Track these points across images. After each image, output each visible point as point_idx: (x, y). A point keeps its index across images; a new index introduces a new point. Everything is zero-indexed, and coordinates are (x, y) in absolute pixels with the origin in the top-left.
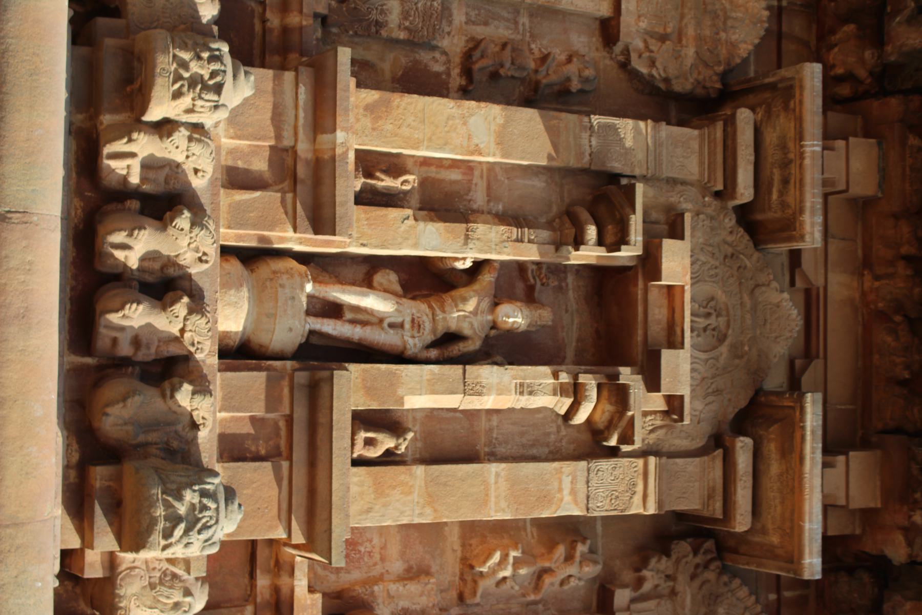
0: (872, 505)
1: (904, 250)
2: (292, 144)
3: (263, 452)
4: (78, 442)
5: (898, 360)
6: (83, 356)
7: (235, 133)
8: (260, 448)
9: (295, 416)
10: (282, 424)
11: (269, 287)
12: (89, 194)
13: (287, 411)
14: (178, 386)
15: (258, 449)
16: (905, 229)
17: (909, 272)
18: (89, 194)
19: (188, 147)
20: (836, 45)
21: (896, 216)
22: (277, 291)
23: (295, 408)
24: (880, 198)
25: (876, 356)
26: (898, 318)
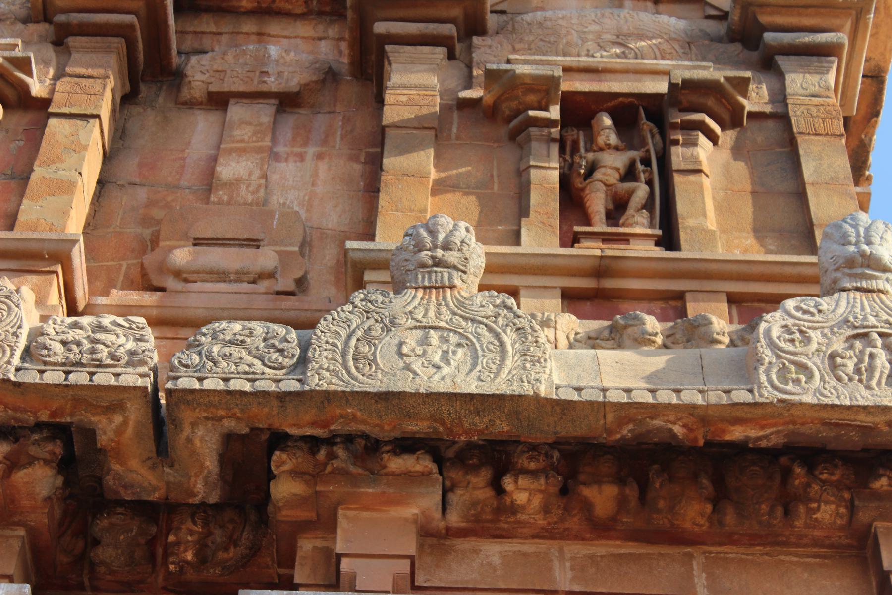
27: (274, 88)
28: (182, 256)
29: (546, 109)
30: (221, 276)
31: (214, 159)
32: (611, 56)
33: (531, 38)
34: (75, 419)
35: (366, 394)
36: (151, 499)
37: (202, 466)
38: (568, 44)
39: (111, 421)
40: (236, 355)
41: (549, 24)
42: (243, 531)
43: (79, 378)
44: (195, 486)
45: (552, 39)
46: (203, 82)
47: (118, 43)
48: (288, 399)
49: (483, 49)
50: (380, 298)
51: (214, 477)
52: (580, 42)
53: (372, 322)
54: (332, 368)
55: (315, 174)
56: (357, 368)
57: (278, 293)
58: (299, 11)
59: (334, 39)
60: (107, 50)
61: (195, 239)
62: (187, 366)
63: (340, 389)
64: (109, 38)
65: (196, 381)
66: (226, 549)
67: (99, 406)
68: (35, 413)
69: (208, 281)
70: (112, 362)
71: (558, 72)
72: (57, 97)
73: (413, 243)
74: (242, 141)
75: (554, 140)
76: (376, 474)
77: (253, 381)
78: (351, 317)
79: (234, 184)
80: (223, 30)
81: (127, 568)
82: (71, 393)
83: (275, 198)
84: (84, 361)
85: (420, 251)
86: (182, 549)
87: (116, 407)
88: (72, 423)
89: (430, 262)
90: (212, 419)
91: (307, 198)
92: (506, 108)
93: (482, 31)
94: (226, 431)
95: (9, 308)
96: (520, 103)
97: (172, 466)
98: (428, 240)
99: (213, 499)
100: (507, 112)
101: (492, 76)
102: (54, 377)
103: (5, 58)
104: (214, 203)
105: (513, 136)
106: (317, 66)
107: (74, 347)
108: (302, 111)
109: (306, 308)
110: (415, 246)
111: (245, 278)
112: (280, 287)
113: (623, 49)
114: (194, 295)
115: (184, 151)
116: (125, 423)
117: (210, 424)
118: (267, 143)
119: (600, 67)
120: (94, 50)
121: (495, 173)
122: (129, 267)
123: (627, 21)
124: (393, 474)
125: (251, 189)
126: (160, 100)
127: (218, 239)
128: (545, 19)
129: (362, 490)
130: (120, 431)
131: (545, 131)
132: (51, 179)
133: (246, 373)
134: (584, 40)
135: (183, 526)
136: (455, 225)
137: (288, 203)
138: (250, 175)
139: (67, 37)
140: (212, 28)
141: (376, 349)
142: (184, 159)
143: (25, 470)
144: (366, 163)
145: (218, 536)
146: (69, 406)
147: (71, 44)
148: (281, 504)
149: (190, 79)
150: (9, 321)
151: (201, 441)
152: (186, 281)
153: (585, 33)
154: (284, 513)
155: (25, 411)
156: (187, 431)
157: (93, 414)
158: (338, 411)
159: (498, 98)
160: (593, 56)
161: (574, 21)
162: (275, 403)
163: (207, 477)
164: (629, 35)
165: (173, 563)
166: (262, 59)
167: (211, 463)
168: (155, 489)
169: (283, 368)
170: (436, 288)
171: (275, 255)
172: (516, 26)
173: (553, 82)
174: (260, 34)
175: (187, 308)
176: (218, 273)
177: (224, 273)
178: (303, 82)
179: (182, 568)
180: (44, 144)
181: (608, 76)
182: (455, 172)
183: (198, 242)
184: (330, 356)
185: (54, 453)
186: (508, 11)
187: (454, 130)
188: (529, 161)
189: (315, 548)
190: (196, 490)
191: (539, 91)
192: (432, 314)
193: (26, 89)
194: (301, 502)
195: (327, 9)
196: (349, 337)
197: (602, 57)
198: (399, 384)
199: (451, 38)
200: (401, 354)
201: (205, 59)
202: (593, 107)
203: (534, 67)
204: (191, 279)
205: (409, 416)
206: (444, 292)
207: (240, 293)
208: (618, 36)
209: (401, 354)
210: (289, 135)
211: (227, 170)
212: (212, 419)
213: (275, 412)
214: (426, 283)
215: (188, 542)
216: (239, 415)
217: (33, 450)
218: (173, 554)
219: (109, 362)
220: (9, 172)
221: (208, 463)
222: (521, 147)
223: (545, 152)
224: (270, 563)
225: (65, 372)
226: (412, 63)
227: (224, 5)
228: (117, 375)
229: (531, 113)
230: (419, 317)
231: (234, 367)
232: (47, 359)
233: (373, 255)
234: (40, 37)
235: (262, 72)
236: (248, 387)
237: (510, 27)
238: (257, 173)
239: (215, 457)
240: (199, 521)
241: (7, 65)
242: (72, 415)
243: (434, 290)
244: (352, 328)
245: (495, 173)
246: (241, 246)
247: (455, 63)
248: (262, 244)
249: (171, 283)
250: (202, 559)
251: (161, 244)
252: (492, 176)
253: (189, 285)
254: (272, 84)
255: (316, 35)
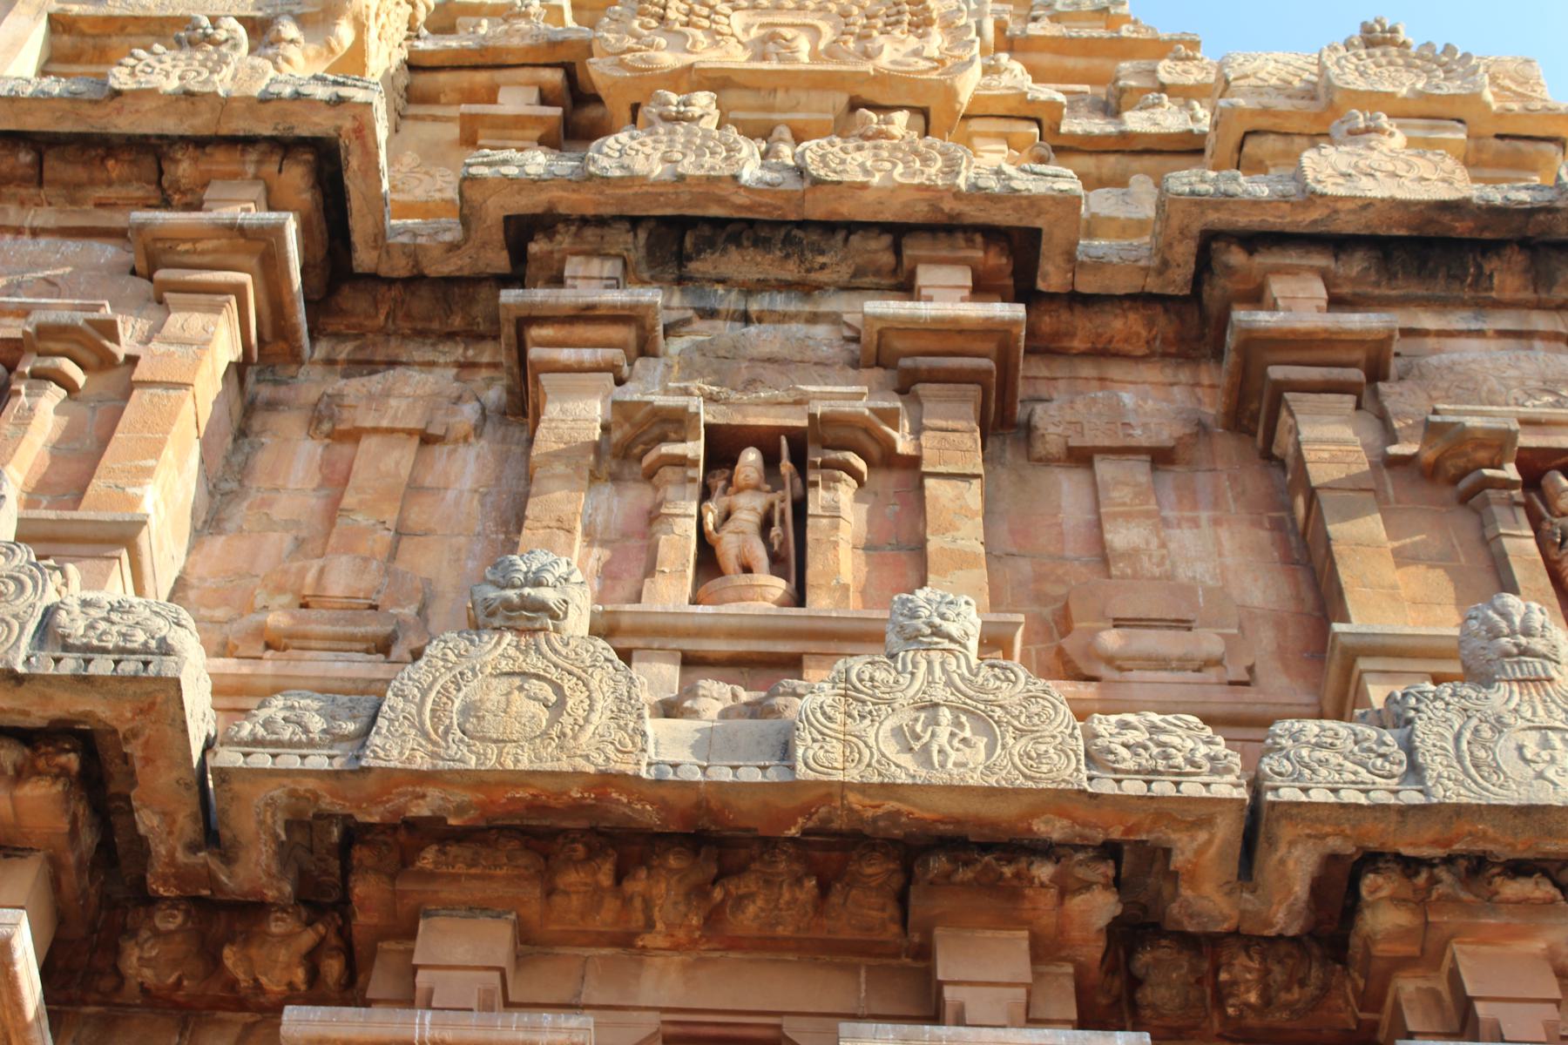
0: (1025, 945)
1: (605, 878)
5: (786, 896)
16: (572, 878)
17: (643, 874)
20: (256, 980)
21: (550, 892)
24: (518, 916)
25: (779, 930)
26: (718, 894)
27: (1145, 443)
28: (1111, 640)
29: (1499, 467)
30: (1160, 663)
31: (1098, 525)
32: (1545, 405)
33: (1446, 385)
34: (1152, 837)
35: (1505, 807)
36: (1218, 930)
37: (1290, 892)
38: (1491, 391)
39: (1193, 839)
40: (1333, 761)
41: (1459, 368)
42: (1310, 968)
43: (1163, 788)
44: (1275, 915)
45: (1470, 385)
46: (1059, 435)
47: (974, 391)
48: (1411, 813)
49: (1393, 398)
50: (1474, 695)
51: (1301, 905)
52: (1503, 389)
53: (1474, 722)
54: (1453, 777)
55: (1218, 542)
56: (1482, 777)
57: (1231, 683)
58: (1139, 353)
59: (1186, 384)
60: (964, 399)
61: (1115, 620)
62: (1280, 774)
63: (1474, 802)
64: (964, 386)
65: (1300, 792)
66: (1288, 989)
67: (1184, 822)
68: (1106, 830)
69: (1146, 669)
70: (1193, 770)
71: (1515, 426)
72: (926, 453)
73: (1484, 628)
74: (1124, 504)
75: (1518, 504)
76: (1492, 901)
77: (1365, 792)
78: (1448, 715)
79: (1132, 555)
80: (1059, 375)
81: (1179, 1012)
82: (1155, 805)
83: (1180, 570)
84: (1161, 768)
85: (1497, 637)
86: (1242, 989)
87: (1205, 822)
88: (1147, 841)
89: (1515, 651)
90: (1315, 837)
91: (1218, 571)
92: (1451, 467)
93: (1385, 378)
94: (1328, 851)
95: (1054, 706)
96: (1469, 461)
97: (1253, 891)
98: (1503, 624)
99: (1293, 931)
100: (1452, 471)
101: (1433, 430)
102: (1133, 787)
103: (871, 409)
104: (1117, 577)
105: (1464, 499)
106: (1184, 416)
107: (1141, 751)
108: (1177, 468)
109: (1274, 701)
110: (1488, 631)
111: (1189, 665)
112: (1232, 677)
113: (1555, 398)
114: (1135, 686)
115: (1055, 515)
116: (1209, 842)
117: (1310, 843)
118: (1153, 506)
119: (1544, 418)
120: (948, 399)
121: (1455, 542)
122: (1038, 653)
123: (1547, 366)
124: (1508, 902)
125: (1154, 560)
126: (1008, 456)
127: (1141, 620)
128: (1454, 363)
129: (1483, 921)
130: (1200, 852)
131: (1505, 493)
132: (952, 551)
133: (1353, 783)
134: (1508, 388)
135: (1236, 962)
136: (1527, 607)
137: (1198, 576)
138: (1148, 543)
139: (915, 383)
140: (1045, 373)
141: (1494, 754)
142: (1060, 525)
143: (1082, 897)
144: (1272, 530)
145: (1278, 974)
146: (1148, 821)
147: (920, 392)
148: (1379, 937)
149: (1041, 432)
150: (1059, 720)
151: (1296, 864)
152: (1120, 669)
153: (1504, 378)
154: (1380, 947)
155: (1095, 826)
156: (1282, 850)
157: (1174, 831)
158: (1467, 828)
159: (1442, 455)
160: (1523, 405)
161: (1488, 365)
162: (1394, 817)
163: (1293, 904)
164: (1558, 381)
165: (1232, 1006)
166: (1118, 408)
167: (1301, 889)
168: (1226, 918)
169: (1392, 776)
170: (1532, 681)
171: (1219, 638)
172: (1424, 370)
173: (1510, 436)
174: (1101, 379)
175: (1133, 701)
176: (1157, 660)
177: (1164, 660)
178: (1176, 435)
179: (1241, 1011)
180: (928, 508)
181: (1554, 429)
182: (1408, 541)
183: (1118, 623)
184: (1445, 763)
185: (1107, 876)
186: (1403, 353)
187: (1391, 491)
188: (1497, 529)
189: (1418, 989)
190: (1275, 920)
191: (1491, 446)
192: (1540, 711)
193: (890, 444)
194: (1404, 934)
195: (1173, 350)
196: (1457, 738)
197: (1534, 406)
198: (1541, 796)
199: (1359, 384)
200: (1527, 761)
201: (1052, 408)
202: (1539, 465)
203: (1485, 419)
204: (1126, 667)
205: (1550, 834)
206: (1543, 685)
207: (1188, 683)
208: (1545, 383)
209: (1527, 761)
210: (1173, 497)
211: (1120, 537)
212: (1315, 837)
213: (1392, 829)
214: (1519, 675)
215: (1247, 981)
216: (1348, 832)
217: (1081, 872)
218: (1231, 995)
219: (1189, 769)
220: (894, 542)
221: (1297, 888)
222: (1477, 511)
223: (1511, 519)
224: (1343, 1006)
225: (1146, 781)
226: (1319, 413)
227: (1053, 346)
228: (1207, 785)
229: (1487, 472)
230: (1528, 715)
231: (1337, 776)
232: (1116, 766)
233: (1367, 640)
234: (880, 384)
235: (1124, 424)
236: (1363, 800)
237: (1416, 371)
238: (1155, 542)
239: (1308, 881)
240: (1256, 957)
241: (873, 418)
242: (1149, 832)
243: (1515, 687)
244: (1456, 727)
245: (1455, 542)
246: (1169, 627)
247: (1361, 413)
248: (1194, 625)
249: (1103, 670)
250: (1267, 1001)
251: (1077, 625)
252: (1453, 546)
253: (1126, 673)
254: (1140, 437)
255: (1166, 380)
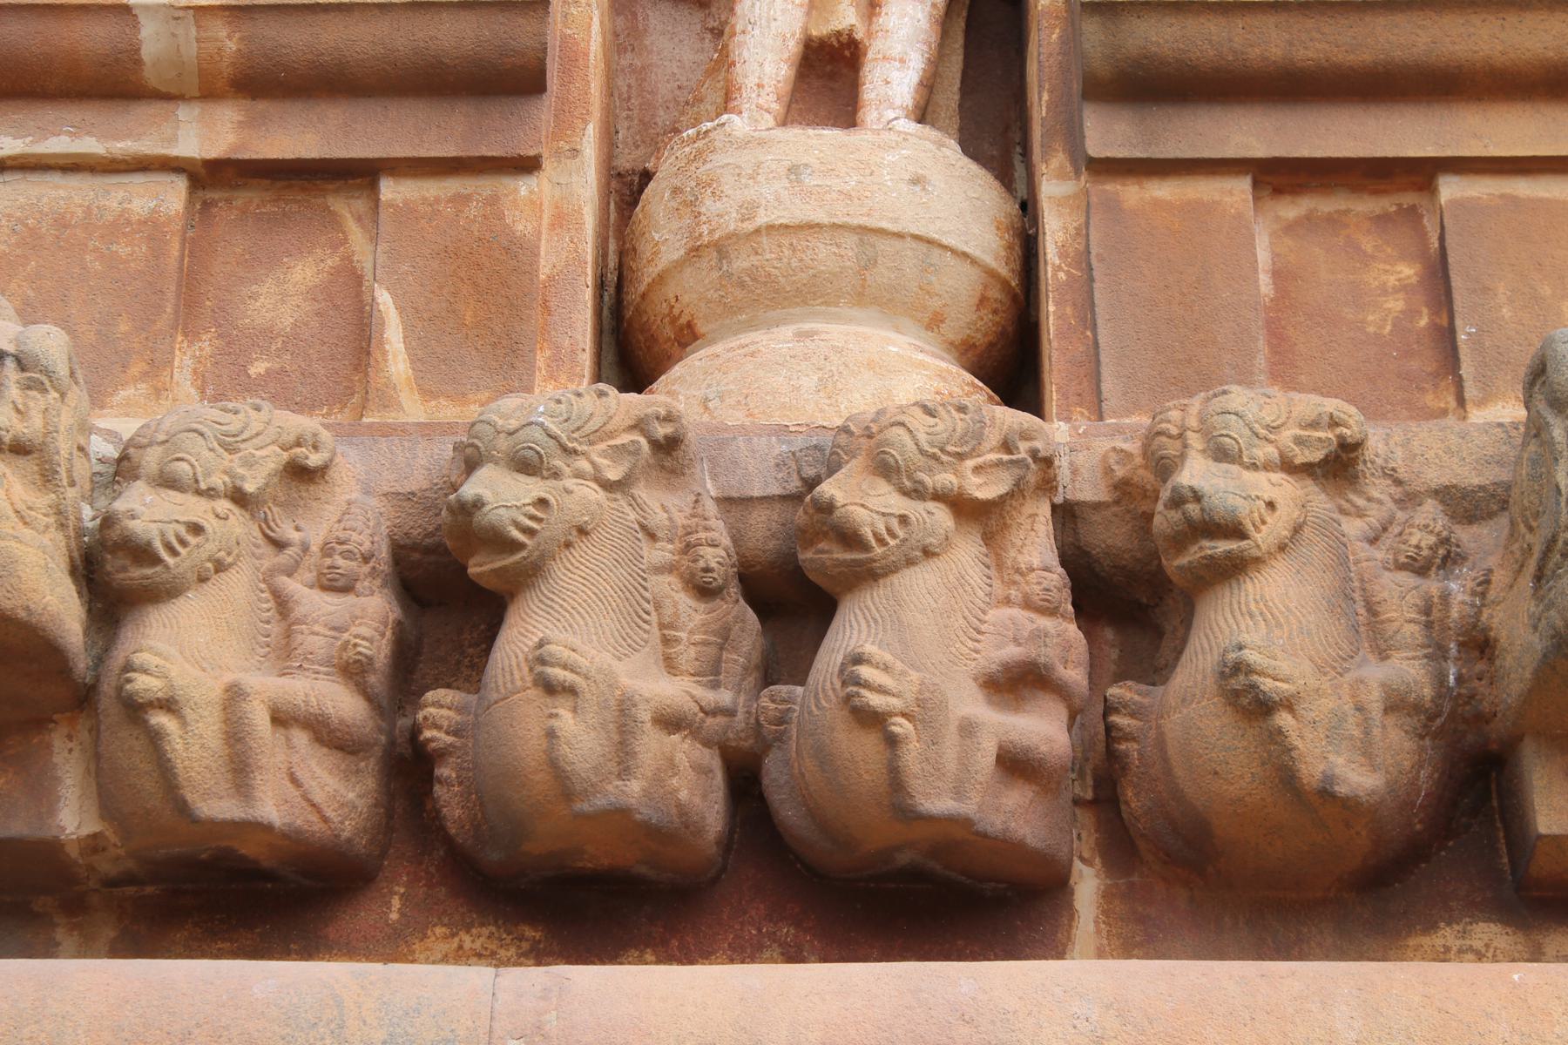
2: (180, 184)
3: (1408, 271)
4: (1430, 927)
6: (1072, 913)
7: (135, 380)
8: (1392, 280)
9: (1260, 151)
10: (1291, 209)
11: (754, 260)
12: (396, 902)
13: (1240, 189)
14: (1192, 509)
15: (1396, 290)
18: (396, 902)
19: (199, 493)
22: (771, 228)
23: (1230, 152)
